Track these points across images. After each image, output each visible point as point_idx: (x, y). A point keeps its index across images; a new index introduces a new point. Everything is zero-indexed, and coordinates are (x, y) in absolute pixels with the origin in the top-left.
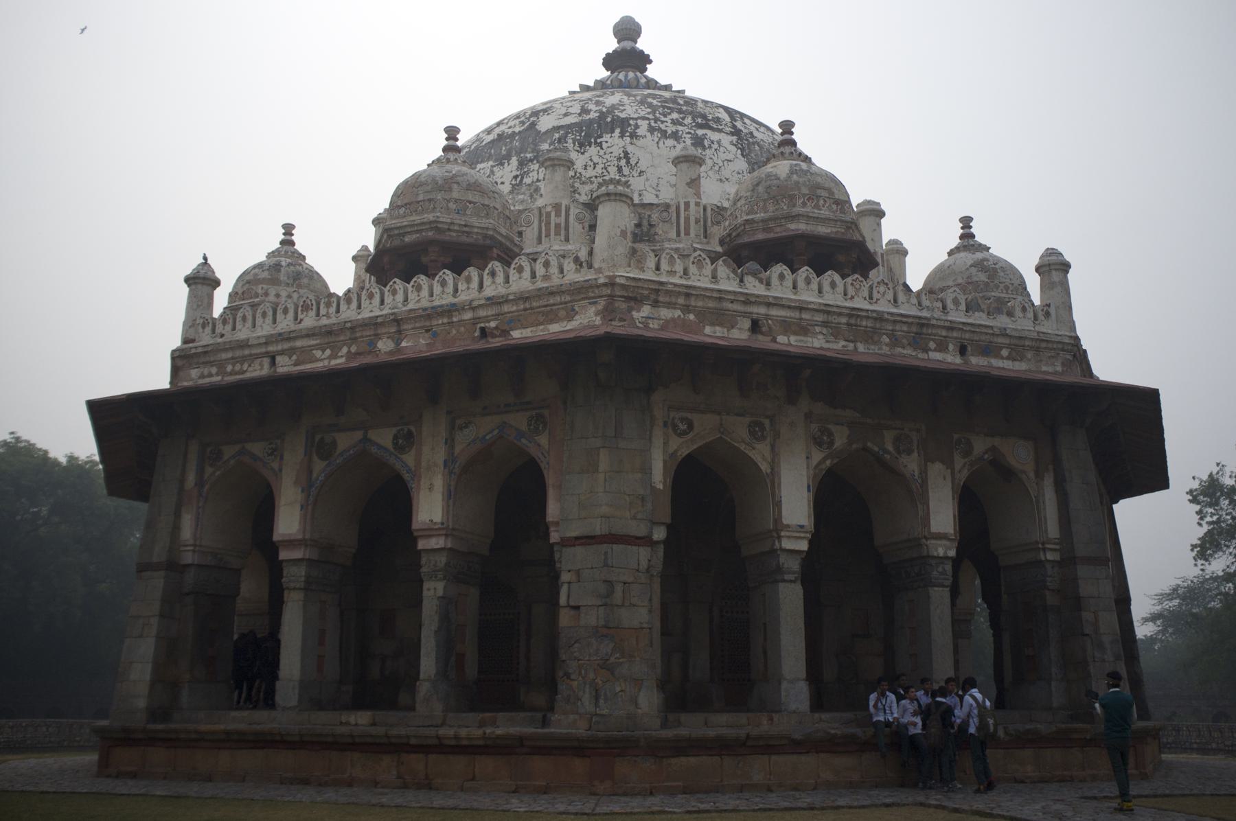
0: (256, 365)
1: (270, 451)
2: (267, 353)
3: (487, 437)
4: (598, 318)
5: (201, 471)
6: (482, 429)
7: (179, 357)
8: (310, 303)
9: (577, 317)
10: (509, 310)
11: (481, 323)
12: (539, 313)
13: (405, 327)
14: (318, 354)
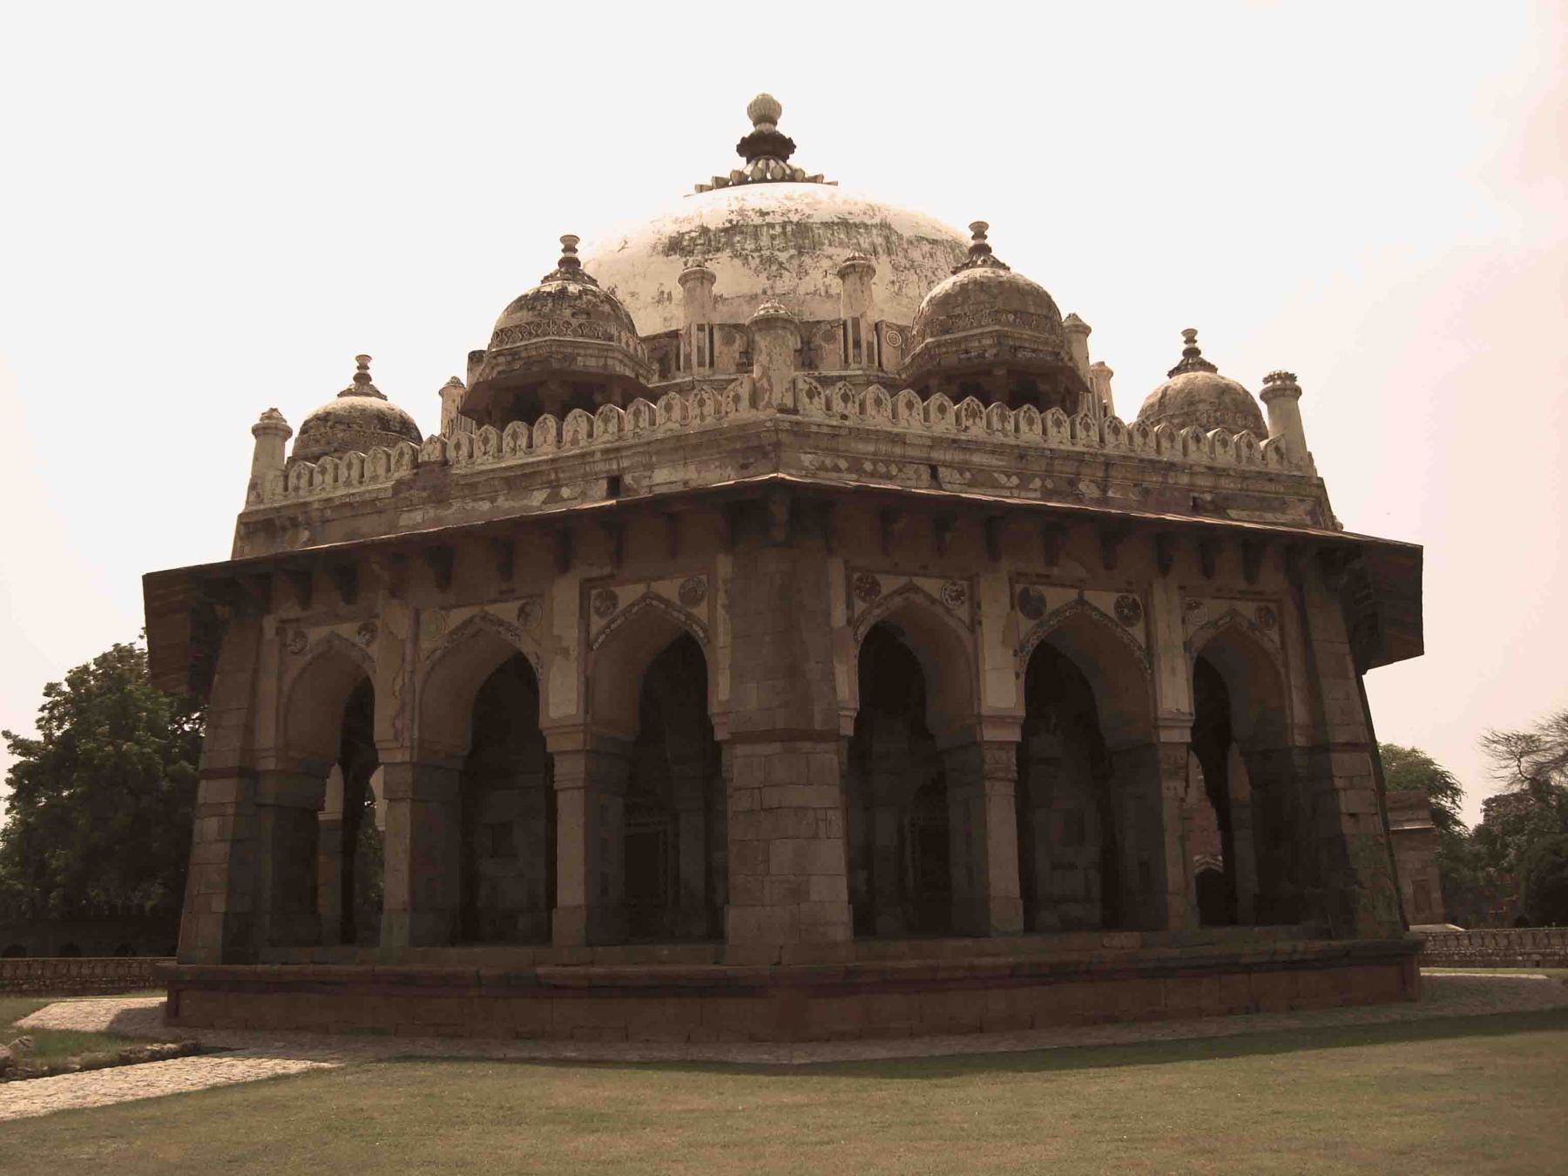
0: (910, 471)
1: (954, 594)
2: (929, 459)
3: (1221, 622)
4: (1308, 518)
5: (850, 606)
6: (1212, 609)
7: (787, 431)
8: (976, 407)
9: (1288, 512)
10: (1227, 486)
11: (1197, 492)
12: (1254, 497)
13: (1114, 473)
14: (1006, 479)
